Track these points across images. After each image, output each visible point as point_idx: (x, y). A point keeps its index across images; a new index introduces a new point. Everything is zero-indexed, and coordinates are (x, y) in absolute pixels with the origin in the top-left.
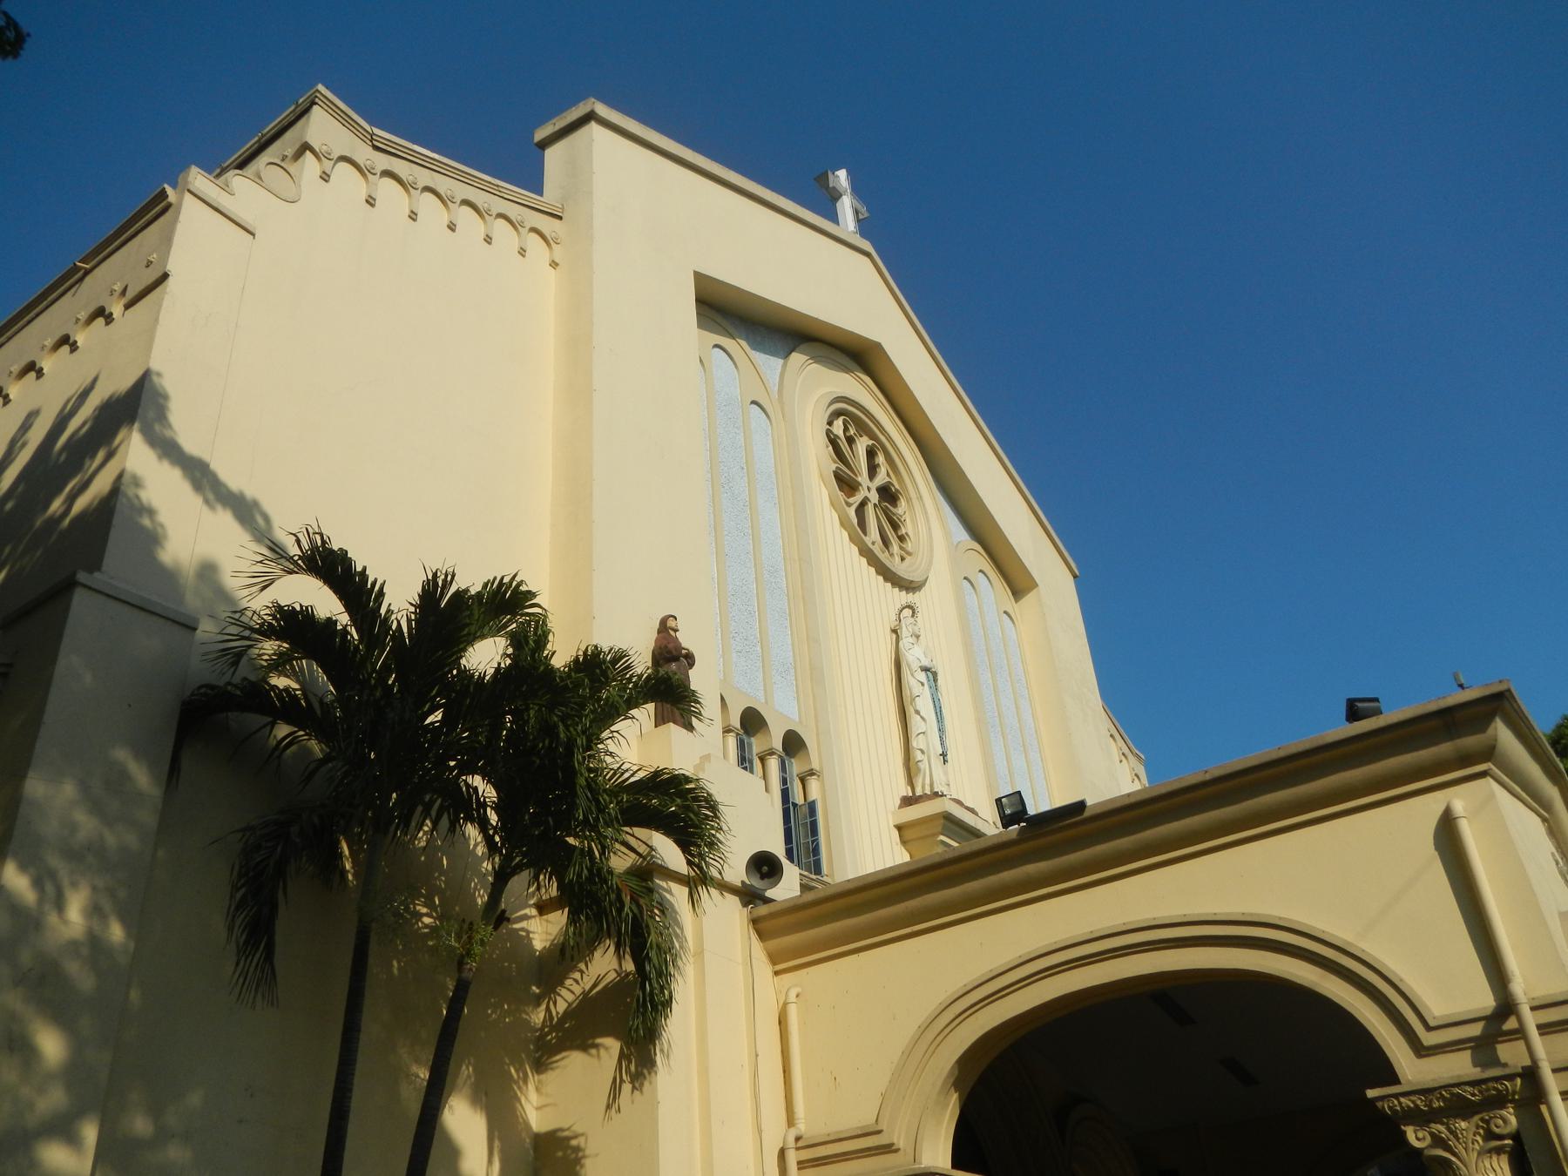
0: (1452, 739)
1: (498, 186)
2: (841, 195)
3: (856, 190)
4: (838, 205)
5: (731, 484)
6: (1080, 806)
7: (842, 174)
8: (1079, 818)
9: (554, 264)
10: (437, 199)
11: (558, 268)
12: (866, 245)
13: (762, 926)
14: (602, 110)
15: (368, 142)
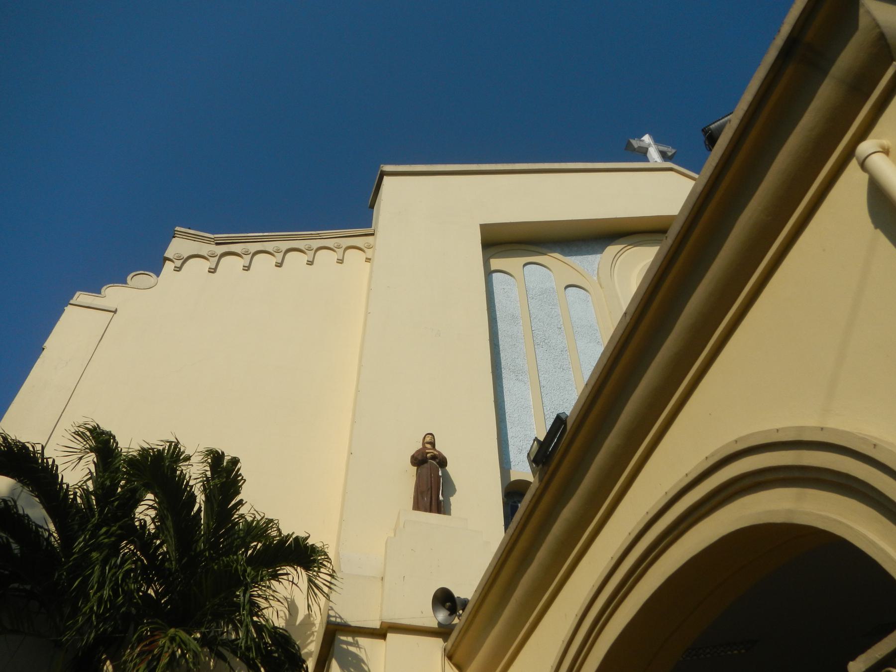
0: (825, 73)
1: (318, 234)
2: (647, 149)
3: (657, 141)
4: (648, 155)
5: (546, 341)
6: (560, 421)
7: (647, 139)
8: (567, 433)
9: (368, 260)
10: (269, 255)
11: (371, 261)
12: (669, 165)
13: (457, 657)
14: (388, 168)
15: (212, 243)
